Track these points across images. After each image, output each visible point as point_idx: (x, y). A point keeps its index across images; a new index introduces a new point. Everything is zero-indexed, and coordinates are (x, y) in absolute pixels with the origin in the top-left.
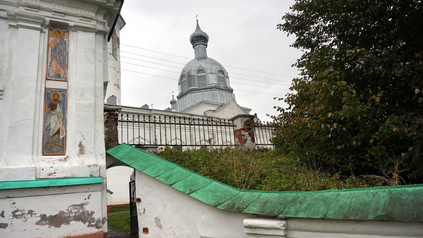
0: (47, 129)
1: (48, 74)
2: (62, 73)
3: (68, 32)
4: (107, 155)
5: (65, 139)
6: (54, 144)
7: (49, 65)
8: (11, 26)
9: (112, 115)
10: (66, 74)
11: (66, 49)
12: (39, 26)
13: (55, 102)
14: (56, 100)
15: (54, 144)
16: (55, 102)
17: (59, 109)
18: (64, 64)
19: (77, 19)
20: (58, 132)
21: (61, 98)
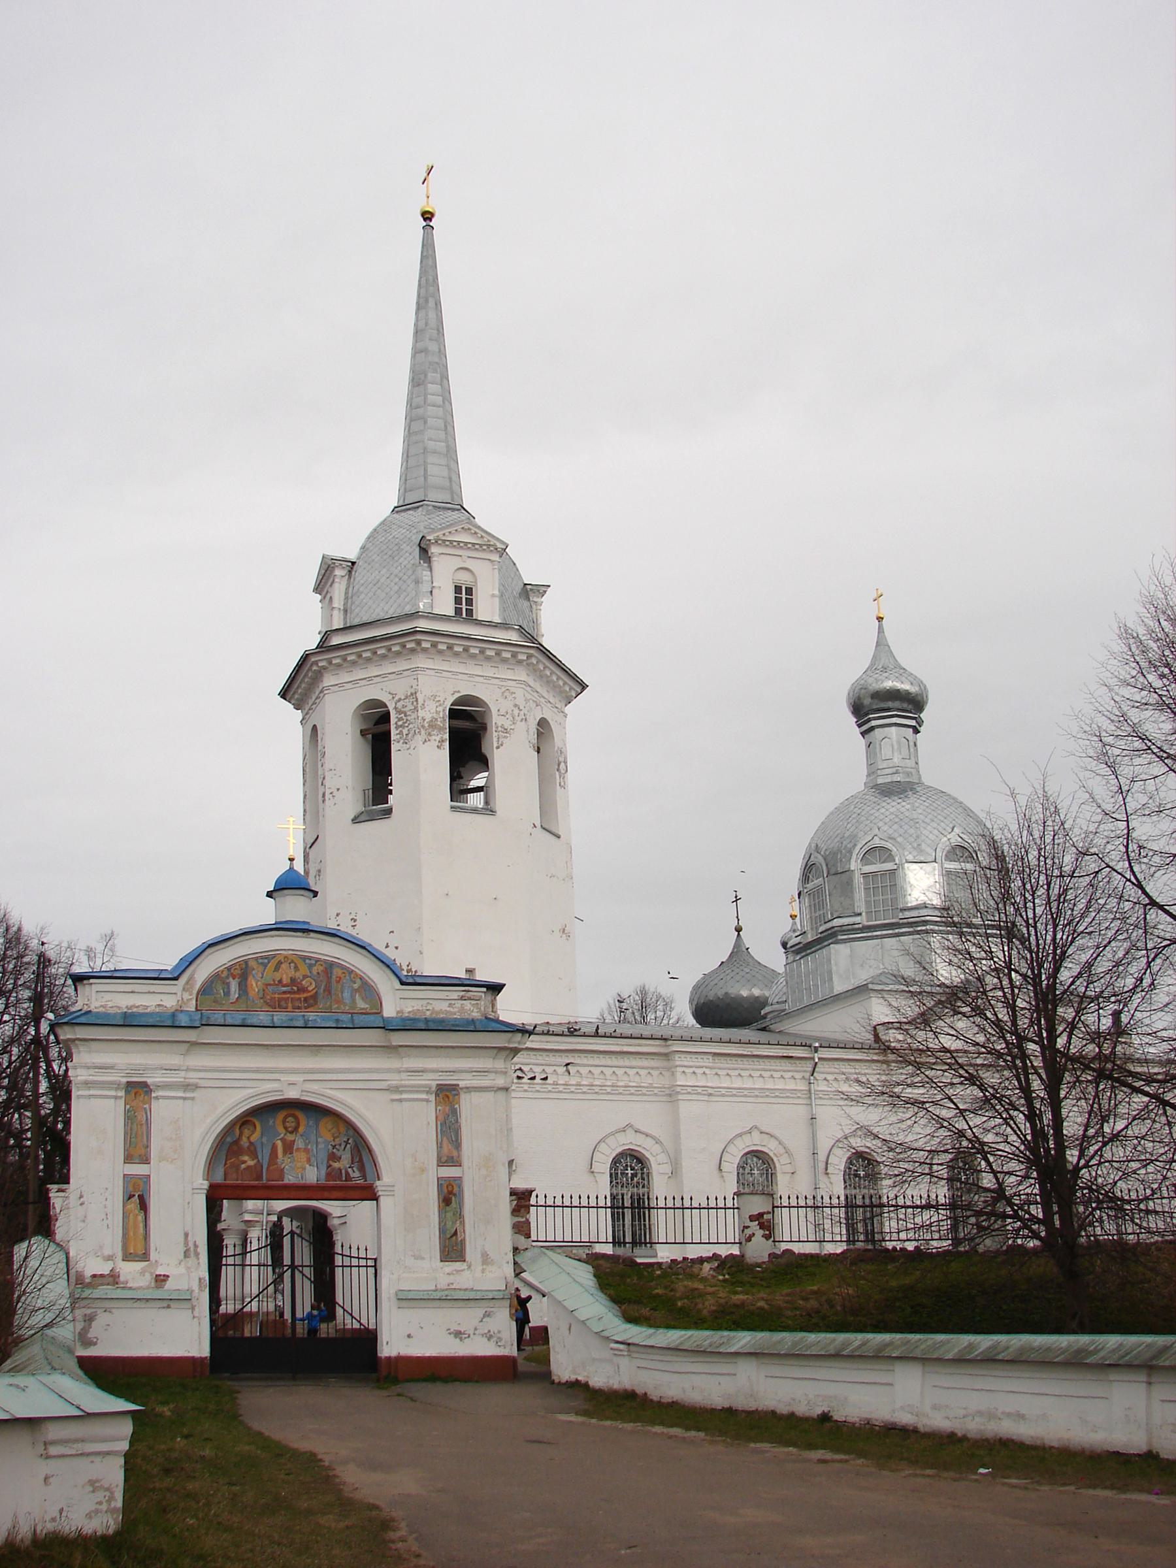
0: (442, 1231)
1: (439, 1159)
2: (455, 1154)
3: (458, 1094)
4: (515, 1263)
5: (463, 1242)
6: (452, 1248)
7: (440, 1146)
8: (393, 1100)
9: (522, 1200)
10: (459, 1156)
11: (457, 1121)
12: (424, 1096)
13: (449, 1195)
14: (451, 1192)
15: (452, 1248)
16: (449, 1195)
17: (453, 1205)
18: (457, 1144)
19: (469, 1076)
20: (455, 1233)
21: (456, 1190)
